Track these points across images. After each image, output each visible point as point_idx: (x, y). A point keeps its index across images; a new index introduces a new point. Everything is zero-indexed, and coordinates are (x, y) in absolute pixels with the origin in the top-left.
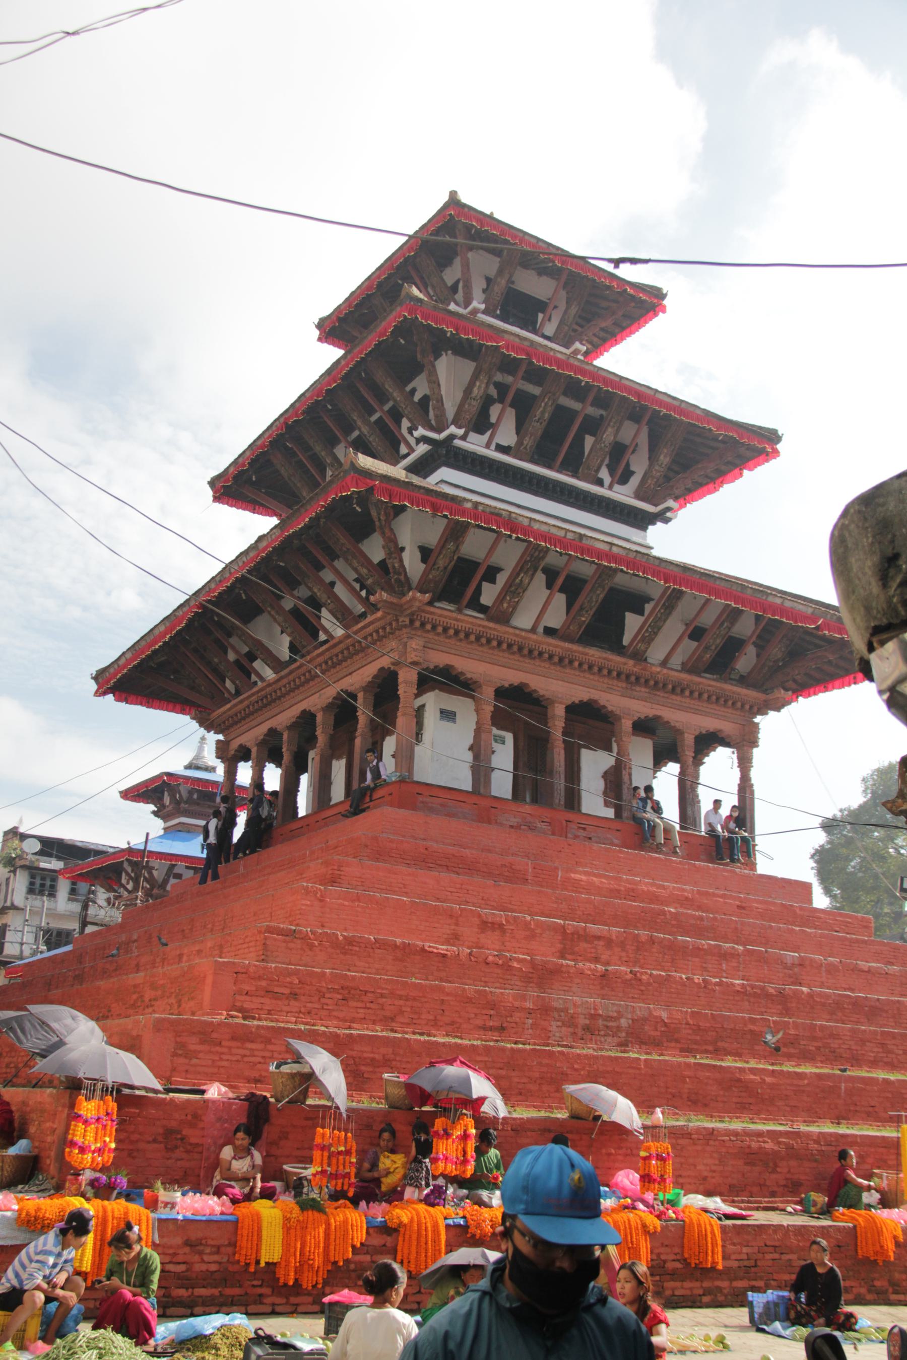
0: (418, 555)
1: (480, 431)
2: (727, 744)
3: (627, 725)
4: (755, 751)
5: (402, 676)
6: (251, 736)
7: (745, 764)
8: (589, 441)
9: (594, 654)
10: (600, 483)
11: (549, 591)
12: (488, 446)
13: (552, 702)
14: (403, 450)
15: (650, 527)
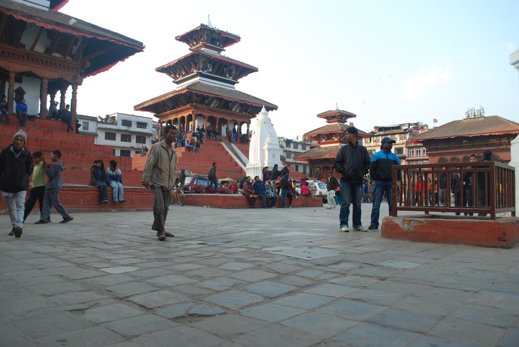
0: (196, 96)
1: (206, 70)
2: (246, 123)
3: (228, 121)
4: (250, 124)
5: (193, 116)
6: (165, 120)
7: (248, 126)
8: (225, 69)
9: (224, 110)
10: (226, 77)
11: (217, 100)
12: (207, 73)
13: (217, 118)
14: (192, 71)
15: (235, 84)
